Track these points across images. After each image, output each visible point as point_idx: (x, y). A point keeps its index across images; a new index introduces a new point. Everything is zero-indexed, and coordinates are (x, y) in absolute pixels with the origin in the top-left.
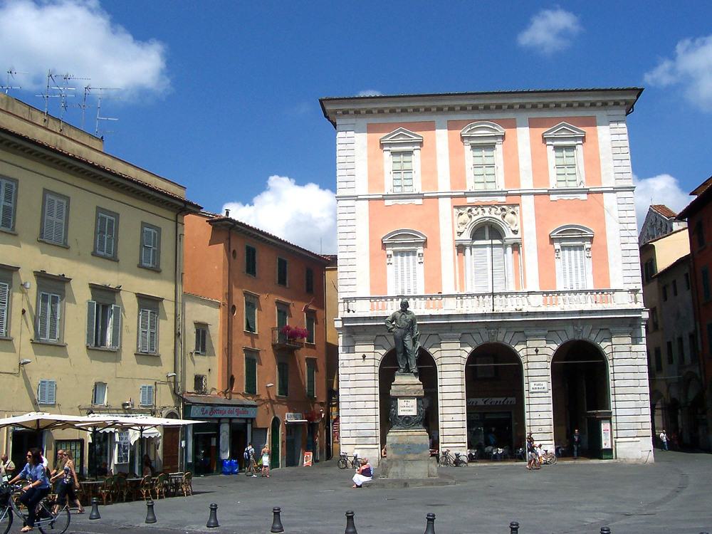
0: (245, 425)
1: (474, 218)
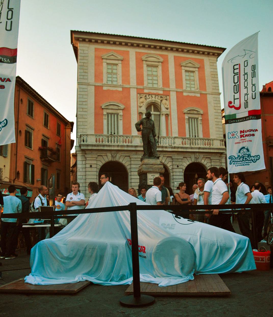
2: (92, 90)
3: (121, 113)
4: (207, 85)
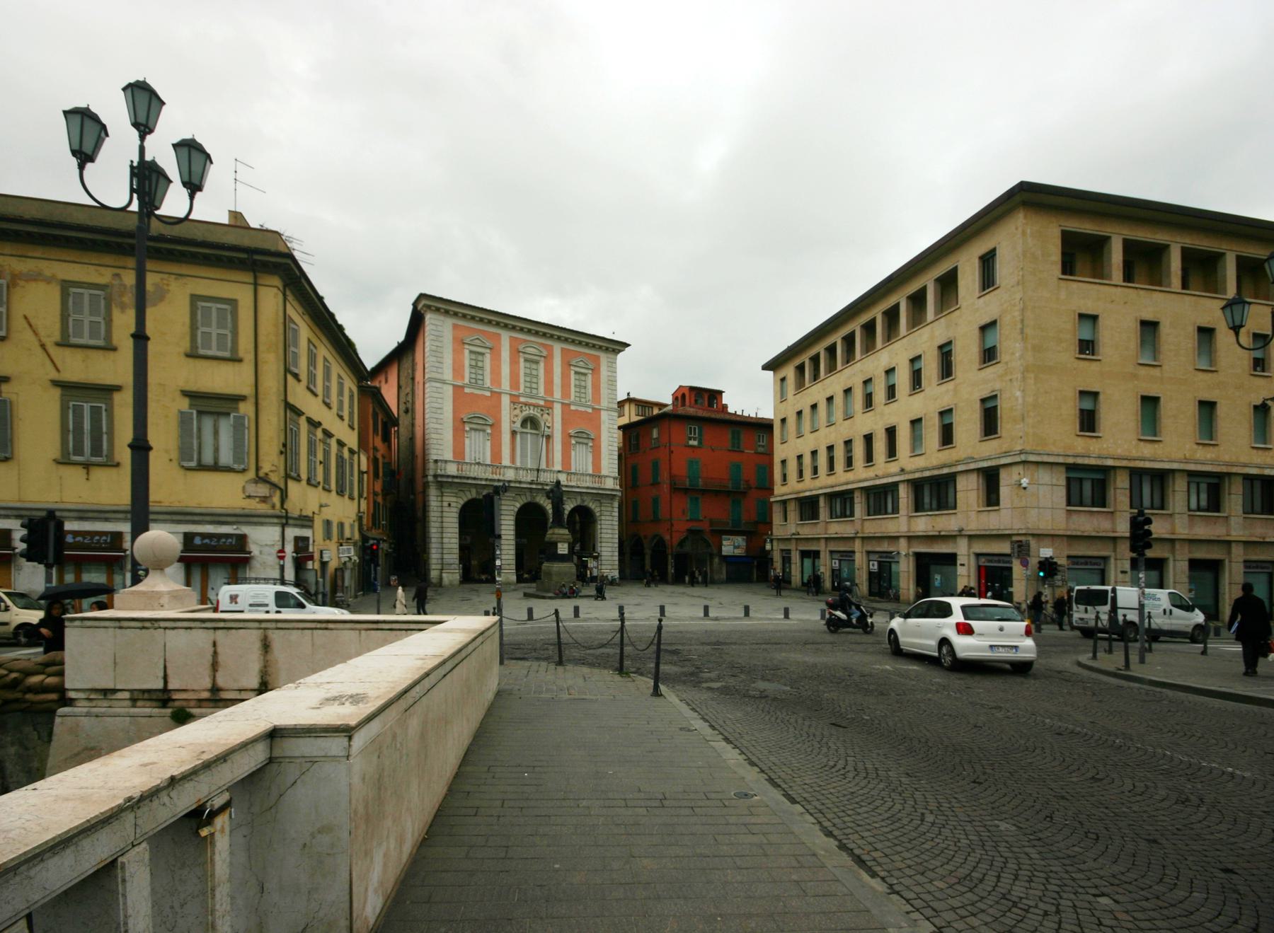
1: (524, 413)
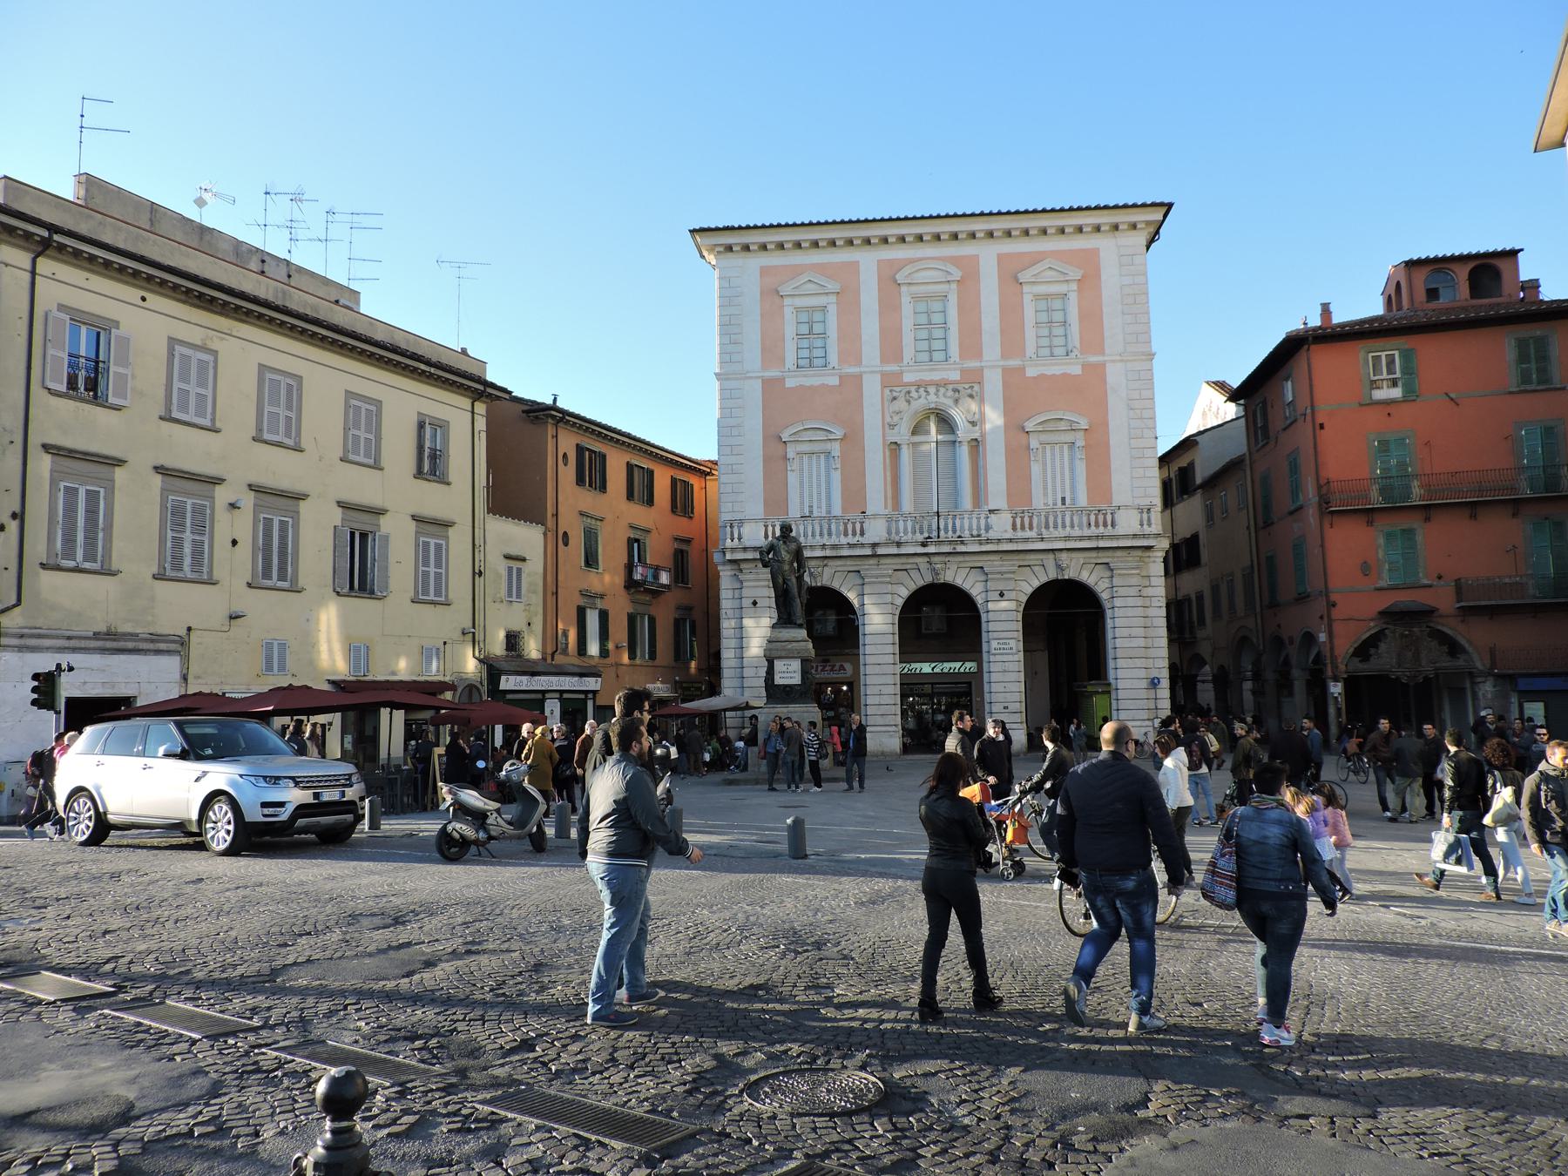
0: (584, 701)
2: (754, 390)
3: (836, 449)
4: (1107, 334)
